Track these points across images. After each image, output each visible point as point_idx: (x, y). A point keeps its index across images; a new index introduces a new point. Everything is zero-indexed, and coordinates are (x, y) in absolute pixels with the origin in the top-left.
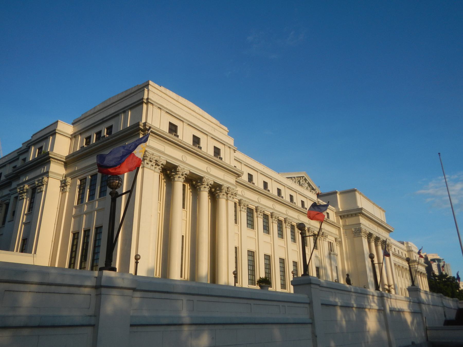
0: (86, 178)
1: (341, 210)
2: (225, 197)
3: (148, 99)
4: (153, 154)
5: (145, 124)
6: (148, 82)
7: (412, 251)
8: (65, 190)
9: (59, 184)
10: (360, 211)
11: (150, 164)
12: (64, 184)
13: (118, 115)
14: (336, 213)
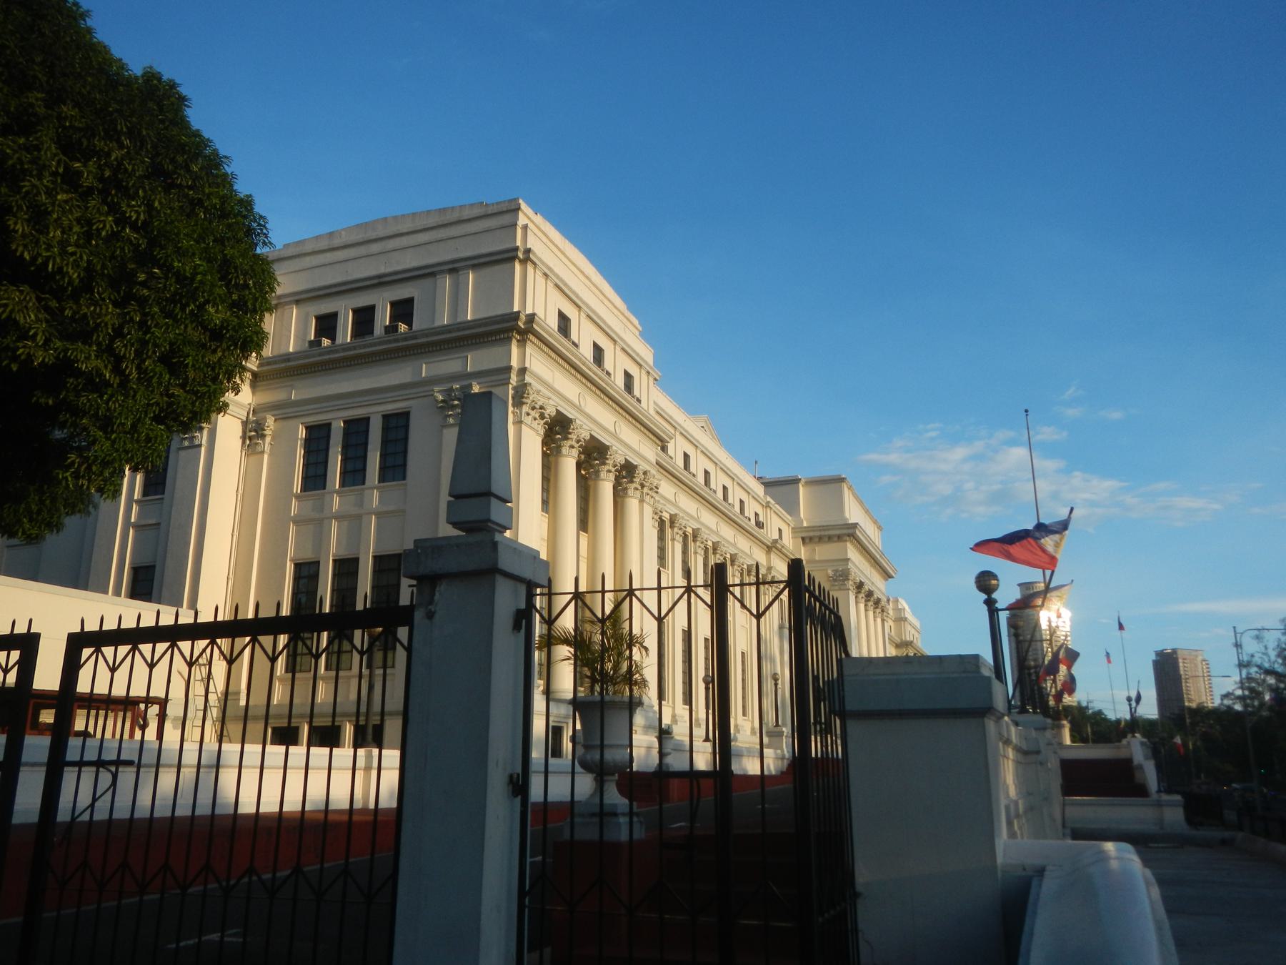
0: (330, 424)
1: (805, 524)
2: (638, 494)
3: (528, 251)
4: (538, 392)
5: (531, 318)
6: (516, 200)
7: (905, 619)
8: (259, 449)
9: (237, 429)
10: (850, 531)
11: (534, 413)
12: (252, 433)
13: (433, 274)
14: (795, 530)
